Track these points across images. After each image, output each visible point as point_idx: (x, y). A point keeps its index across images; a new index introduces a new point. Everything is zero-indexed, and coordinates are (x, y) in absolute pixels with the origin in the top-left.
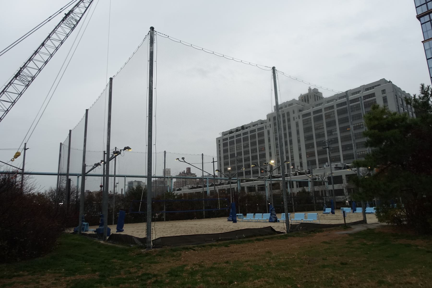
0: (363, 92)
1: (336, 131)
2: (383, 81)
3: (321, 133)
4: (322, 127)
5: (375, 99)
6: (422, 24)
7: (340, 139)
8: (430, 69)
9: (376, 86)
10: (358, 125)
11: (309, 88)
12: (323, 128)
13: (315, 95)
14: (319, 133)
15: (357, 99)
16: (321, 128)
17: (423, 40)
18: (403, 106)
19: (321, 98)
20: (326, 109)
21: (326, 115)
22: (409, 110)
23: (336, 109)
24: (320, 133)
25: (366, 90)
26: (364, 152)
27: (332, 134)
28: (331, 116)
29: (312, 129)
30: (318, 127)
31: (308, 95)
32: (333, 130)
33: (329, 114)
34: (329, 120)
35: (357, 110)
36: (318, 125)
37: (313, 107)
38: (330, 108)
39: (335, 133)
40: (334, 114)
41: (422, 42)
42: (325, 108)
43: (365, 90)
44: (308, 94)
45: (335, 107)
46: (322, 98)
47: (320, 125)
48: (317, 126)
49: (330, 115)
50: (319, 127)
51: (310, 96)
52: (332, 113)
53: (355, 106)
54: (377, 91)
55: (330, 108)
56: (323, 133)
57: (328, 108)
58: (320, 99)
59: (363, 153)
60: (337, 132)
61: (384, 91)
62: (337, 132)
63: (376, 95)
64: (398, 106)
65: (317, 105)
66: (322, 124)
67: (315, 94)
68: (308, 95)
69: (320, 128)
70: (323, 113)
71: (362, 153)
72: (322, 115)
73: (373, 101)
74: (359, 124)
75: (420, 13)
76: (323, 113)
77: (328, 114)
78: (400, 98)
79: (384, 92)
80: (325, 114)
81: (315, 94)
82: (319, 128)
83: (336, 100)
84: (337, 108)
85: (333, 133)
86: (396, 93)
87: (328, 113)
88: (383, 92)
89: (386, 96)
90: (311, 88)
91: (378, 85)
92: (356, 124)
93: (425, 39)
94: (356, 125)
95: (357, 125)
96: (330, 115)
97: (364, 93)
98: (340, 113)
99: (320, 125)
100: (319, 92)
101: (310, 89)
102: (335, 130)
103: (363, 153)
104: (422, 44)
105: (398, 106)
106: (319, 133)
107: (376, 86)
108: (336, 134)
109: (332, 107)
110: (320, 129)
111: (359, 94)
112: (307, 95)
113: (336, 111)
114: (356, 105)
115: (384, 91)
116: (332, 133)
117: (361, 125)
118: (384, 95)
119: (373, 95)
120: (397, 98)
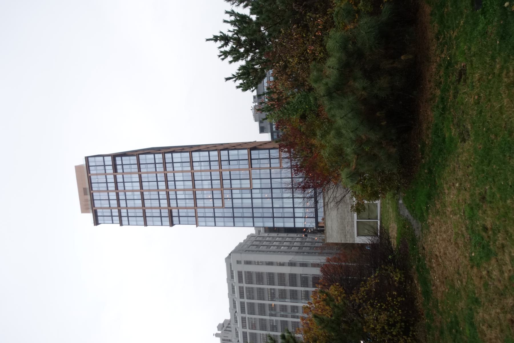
0: (234, 283)
1: (273, 320)
2: (228, 259)
5: (245, 272)
6: (180, 224)
7: (283, 318)
8: (226, 226)
9: (231, 268)
10: (271, 294)
11: (215, 336)
13: (225, 330)
15: (240, 290)
17: (196, 225)
18: (258, 245)
19: (229, 326)
20: (244, 326)
21: (251, 328)
22: (264, 240)
23: (247, 316)
25: (233, 278)
26: (303, 295)
28: (253, 322)
31: (223, 339)
33: (250, 324)
34: (258, 326)
35: (253, 293)
36: (262, 340)
37: (238, 341)
38: (244, 322)
39: (275, 322)
40: (251, 318)
41: (197, 226)
42: (243, 328)
43: (232, 279)
44: (221, 339)
45: (243, 315)
46: (230, 321)
49: (252, 323)
50: (264, 339)
51: (224, 337)
52: (250, 320)
53: (248, 294)
54: (237, 268)
55: (244, 322)
57: (244, 324)
58: (230, 327)
59: (304, 296)
60: (274, 320)
61: (238, 262)
62: (274, 320)
63: (240, 270)
64: (257, 251)
65: (237, 336)
66: (261, 336)
67: (224, 329)
68: (223, 339)
70: (248, 331)
71: (303, 295)
72: (250, 334)
73: (246, 274)
74: (269, 293)
75: (168, 223)
76: (248, 331)
77: (250, 326)
78: (250, 247)
79: (239, 262)
80: (250, 329)
81: (224, 328)
83: (236, 312)
84: (245, 314)
85: (275, 324)
86: (243, 250)
87: (249, 325)
88: (239, 263)
90: (215, 333)
91: (231, 266)
93: (195, 223)
94: (270, 297)
95: (269, 295)
96: (252, 323)
97: (235, 281)
98: (252, 311)
99: (262, 338)
100: (223, 324)
101: (217, 335)
102: (271, 322)
103: (304, 296)
104: (198, 227)
105: (257, 251)
107: (231, 268)
108: (276, 321)
109: (243, 319)
111: (235, 286)
112: (223, 341)
113: (249, 315)
114: (247, 292)
115: (238, 262)
117: (271, 292)
118: (243, 262)
119: (240, 274)
120: (249, 251)
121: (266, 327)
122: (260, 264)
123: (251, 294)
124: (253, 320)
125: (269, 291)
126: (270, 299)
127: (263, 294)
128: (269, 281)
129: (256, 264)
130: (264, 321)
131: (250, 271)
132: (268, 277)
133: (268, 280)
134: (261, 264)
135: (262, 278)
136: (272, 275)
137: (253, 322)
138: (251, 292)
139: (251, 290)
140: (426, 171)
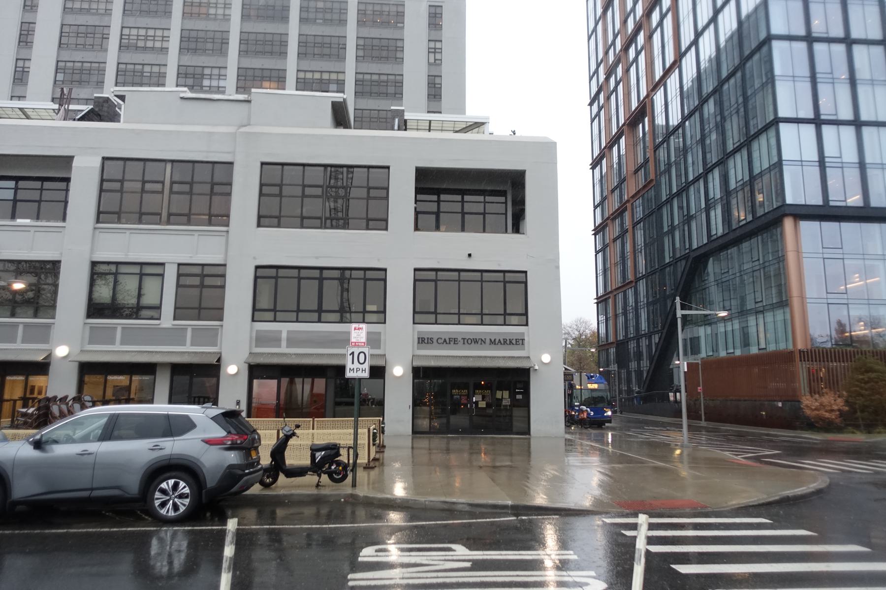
3: (147, 69)
4: (158, 45)
10: (321, 80)
12: (164, 50)
14: (140, 67)
16: (153, 48)
24: (143, 65)
27: (202, 87)
28: (212, 11)
29: (105, 37)
30: (138, 39)
32: (207, 71)
36: (142, 32)
39: (214, 83)
47: (151, 33)
48: (134, 32)
50: (146, 36)
56: (156, 69)
62: (222, 83)
66: (159, 33)
69: (150, 44)
74: (326, 76)
82: (141, 44)
85: (206, 83)
89: (442, 6)
92: (313, 71)
94: (309, 75)
99: (151, 33)
102: (216, 71)
106: (139, 67)
110: (145, 48)
116: (202, 83)
121: (195, 51)
122: (432, 55)
123: (320, 15)
124: (220, 11)
125: (334, 76)
126: (301, 75)
127: (322, 56)
128: (372, 81)
129: (432, 45)
130: (218, 46)
131: (407, 20)
132: (384, 78)
133: (375, 77)
134: (432, 60)
135: (379, 59)
136: (391, 90)
137: (212, 11)
138: (328, 16)
139: (336, 17)
140: (687, 587)
